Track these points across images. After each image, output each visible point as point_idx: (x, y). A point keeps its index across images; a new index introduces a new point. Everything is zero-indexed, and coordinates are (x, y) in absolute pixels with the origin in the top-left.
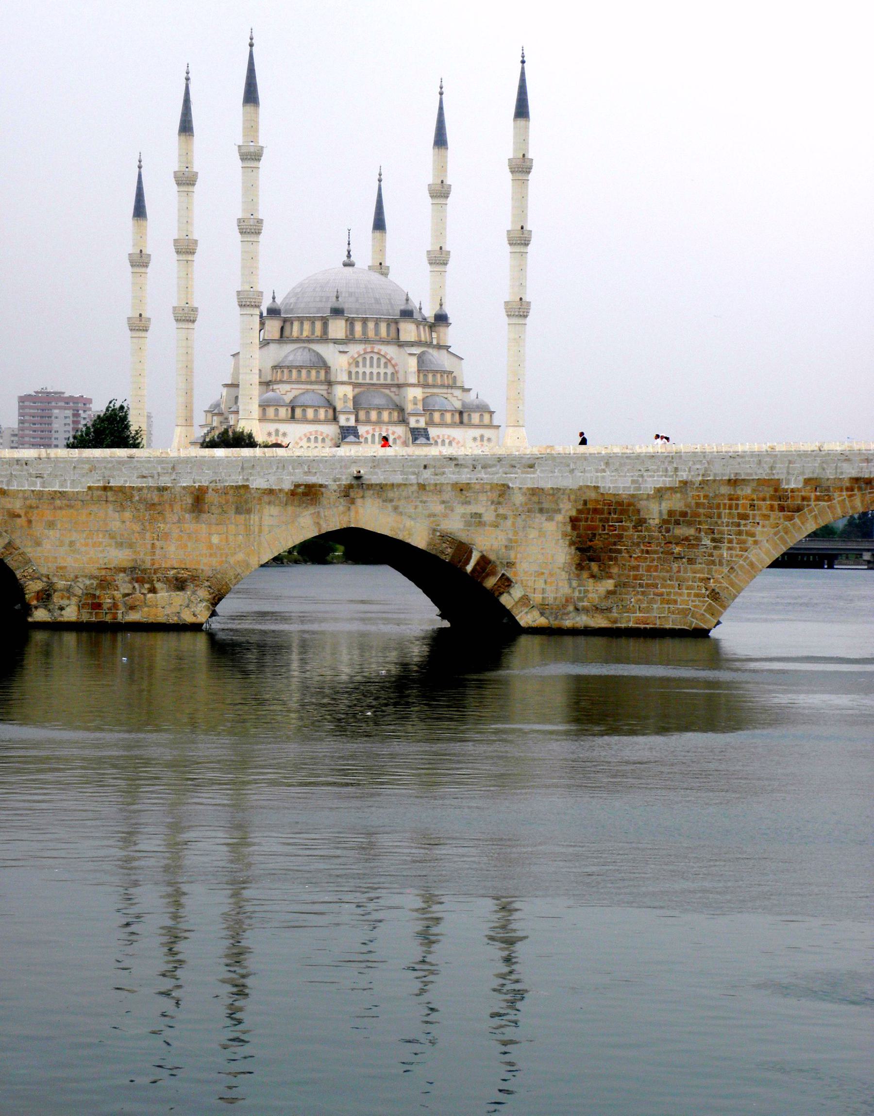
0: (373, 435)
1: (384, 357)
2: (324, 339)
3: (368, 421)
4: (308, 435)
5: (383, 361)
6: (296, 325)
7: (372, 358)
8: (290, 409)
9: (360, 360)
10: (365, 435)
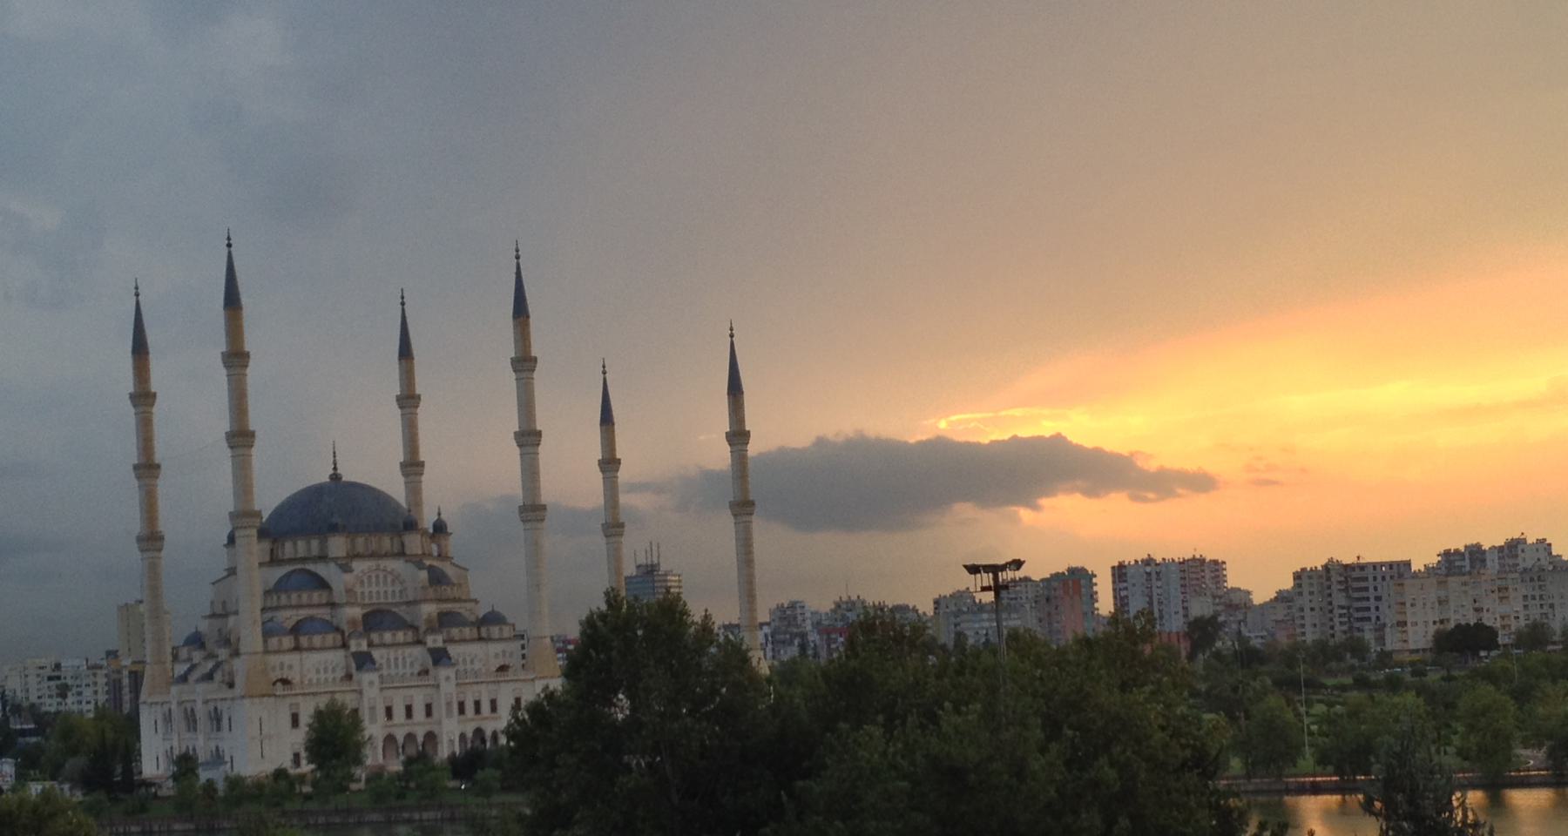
2: (323, 558)
3: (384, 645)
6: (288, 546)
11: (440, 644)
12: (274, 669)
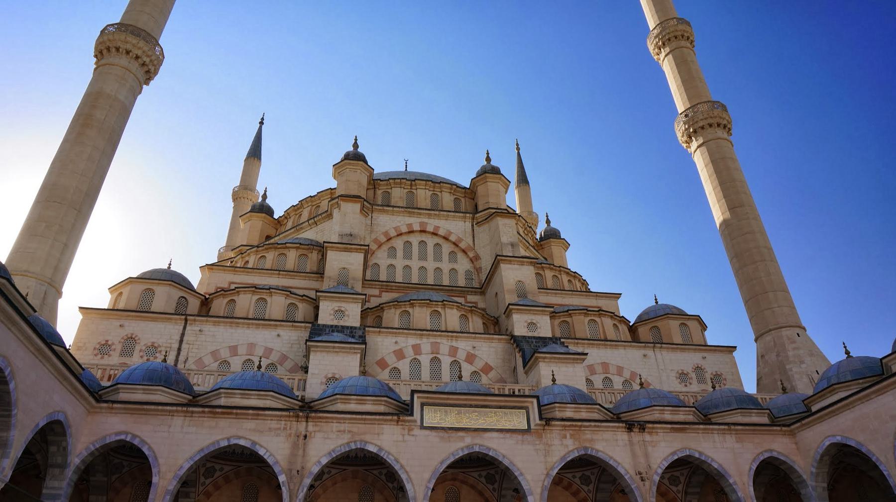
0: (416, 363)
1: (446, 238)
4: (225, 354)
5: (446, 248)
7: (422, 243)
9: (399, 244)
10: (392, 361)
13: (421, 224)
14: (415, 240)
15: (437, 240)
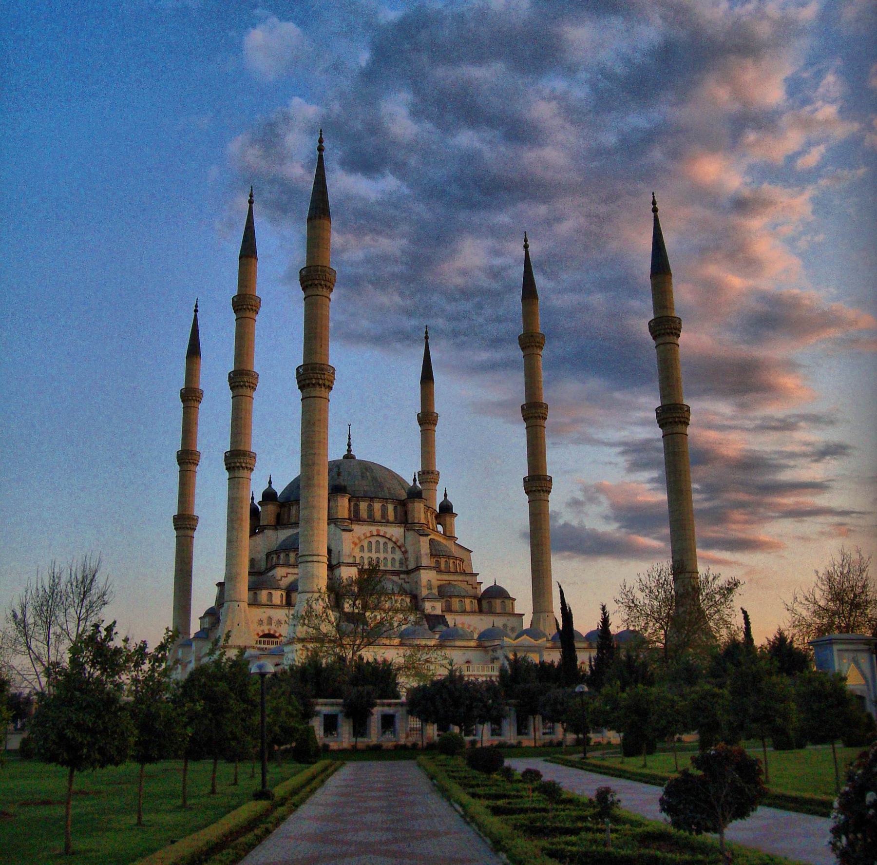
1: (390, 539)
8: (284, 594)
11: (438, 612)
12: (261, 622)
13: (378, 531)
14: (373, 540)
15: (384, 540)
